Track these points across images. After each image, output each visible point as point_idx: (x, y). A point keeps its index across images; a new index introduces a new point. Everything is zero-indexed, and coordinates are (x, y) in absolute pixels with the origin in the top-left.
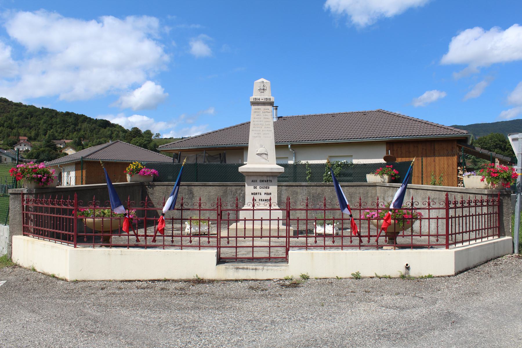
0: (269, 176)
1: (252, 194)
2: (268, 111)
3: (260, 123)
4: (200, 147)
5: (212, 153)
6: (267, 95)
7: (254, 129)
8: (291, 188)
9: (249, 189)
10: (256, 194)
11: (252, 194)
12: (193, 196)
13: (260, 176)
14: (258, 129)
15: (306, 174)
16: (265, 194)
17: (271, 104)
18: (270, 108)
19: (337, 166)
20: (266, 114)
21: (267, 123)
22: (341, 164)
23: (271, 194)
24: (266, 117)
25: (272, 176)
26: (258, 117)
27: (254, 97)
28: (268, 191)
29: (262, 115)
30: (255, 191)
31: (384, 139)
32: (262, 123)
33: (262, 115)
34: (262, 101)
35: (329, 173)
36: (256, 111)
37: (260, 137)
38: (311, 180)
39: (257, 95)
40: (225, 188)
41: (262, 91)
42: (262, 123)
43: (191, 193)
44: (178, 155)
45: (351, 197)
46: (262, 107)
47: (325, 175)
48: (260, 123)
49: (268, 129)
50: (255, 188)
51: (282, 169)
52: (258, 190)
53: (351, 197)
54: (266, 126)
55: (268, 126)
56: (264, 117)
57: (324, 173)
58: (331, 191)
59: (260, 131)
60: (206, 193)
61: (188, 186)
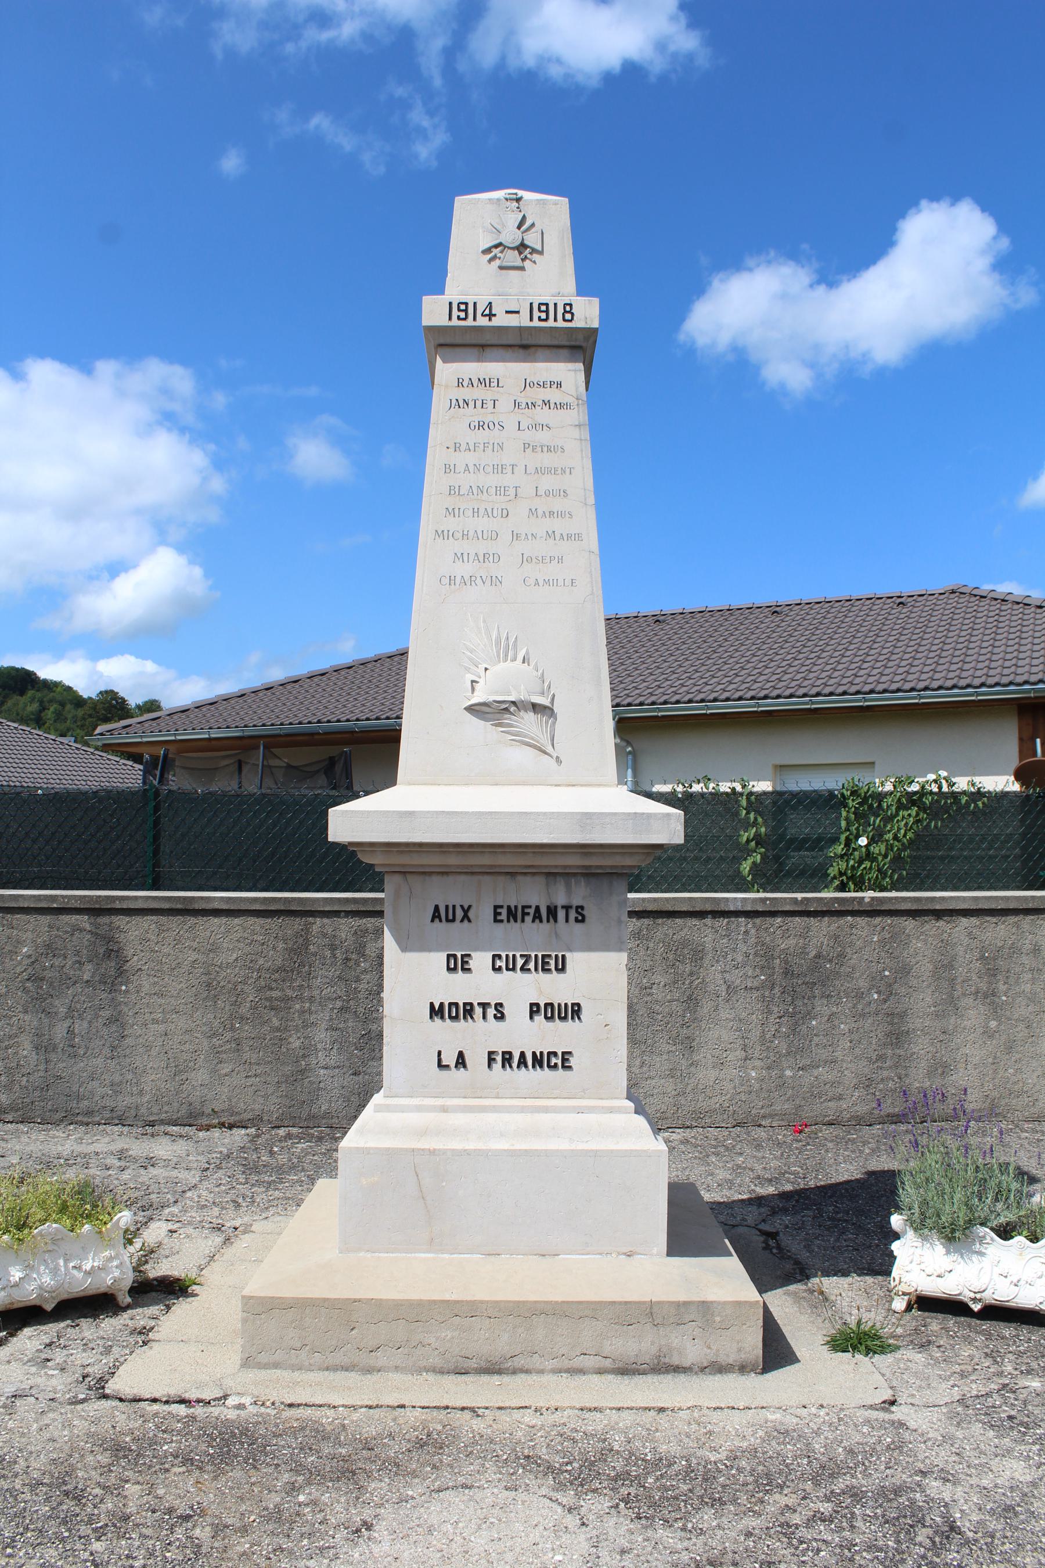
0: (567, 875)
1: (436, 1012)
2: (554, 395)
3: (491, 480)
4: (249, 732)
5: (301, 757)
6: (550, 281)
7: (451, 524)
8: (666, 928)
9: (411, 976)
10: (468, 1010)
11: (436, 1012)
12: (120, 972)
13: (492, 872)
14: (483, 524)
15: (738, 844)
16: (534, 1009)
17: (578, 346)
18: (569, 374)
19: (900, 806)
20: (542, 415)
21: (547, 482)
22: (923, 793)
23: (576, 1011)
24: (542, 437)
25: (589, 875)
26: (482, 435)
27: (454, 292)
28: (555, 988)
29: (510, 423)
30: (458, 989)
31: (1012, 693)
32: (507, 480)
33: (510, 423)
34: (512, 321)
35: (863, 841)
36: (466, 393)
37: (495, 581)
38: (764, 878)
39: (470, 281)
40: (297, 923)
41: (512, 258)
42: (507, 480)
43: (109, 954)
44: (158, 761)
45: (992, 973)
46: (510, 372)
47: (839, 849)
48: (491, 480)
49: (558, 525)
50: (458, 964)
51: (667, 827)
52: (482, 982)
53: (992, 973)
54: (542, 505)
55: (557, 504)
56: (528, 436)
57: (835, 840)
58: (883, 942)
59: (495, 536)
60: (187, 953)
61: (96, 911)
